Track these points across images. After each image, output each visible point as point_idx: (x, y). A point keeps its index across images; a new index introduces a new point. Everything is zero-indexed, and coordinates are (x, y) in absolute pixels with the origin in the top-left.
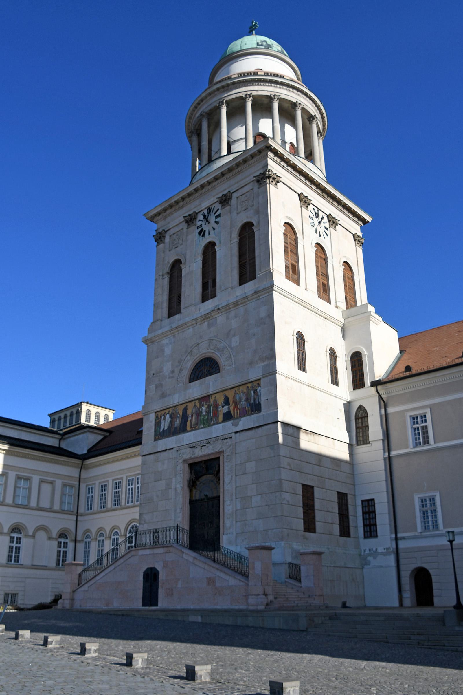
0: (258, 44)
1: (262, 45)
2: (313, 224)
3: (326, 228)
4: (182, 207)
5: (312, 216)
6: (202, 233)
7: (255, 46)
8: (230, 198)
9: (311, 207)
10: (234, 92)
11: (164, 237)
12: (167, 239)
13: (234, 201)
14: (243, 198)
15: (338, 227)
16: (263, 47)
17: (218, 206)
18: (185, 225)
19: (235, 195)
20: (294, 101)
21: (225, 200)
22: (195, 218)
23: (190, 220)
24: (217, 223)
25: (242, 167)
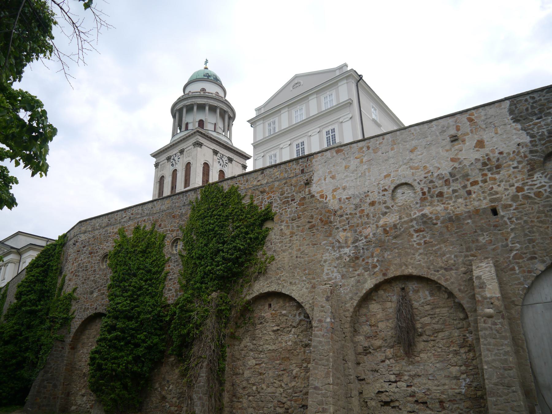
0: (204, 76)
1: (206, 76)
2: (219, 162)
3: (226, 163)
4: (165, 153)
5: (219, 158)
6: (172, 165)
7: (203, 77)
8: (183, 151)
9: (219, 155)
10: (190, 101)
11: (158, 165)
12: (159, 167)
13: (185, 153)
14: (188, 152)
15: (233, 162)
16: (206, 77)
17: (179, 154)
18: (166, 161)
19: (185, 150)
20: (216, 105)
21: (182, 152)
22: (170, 158)
23: (169, 159)
24: (178, 161)
25: (189, 138)
